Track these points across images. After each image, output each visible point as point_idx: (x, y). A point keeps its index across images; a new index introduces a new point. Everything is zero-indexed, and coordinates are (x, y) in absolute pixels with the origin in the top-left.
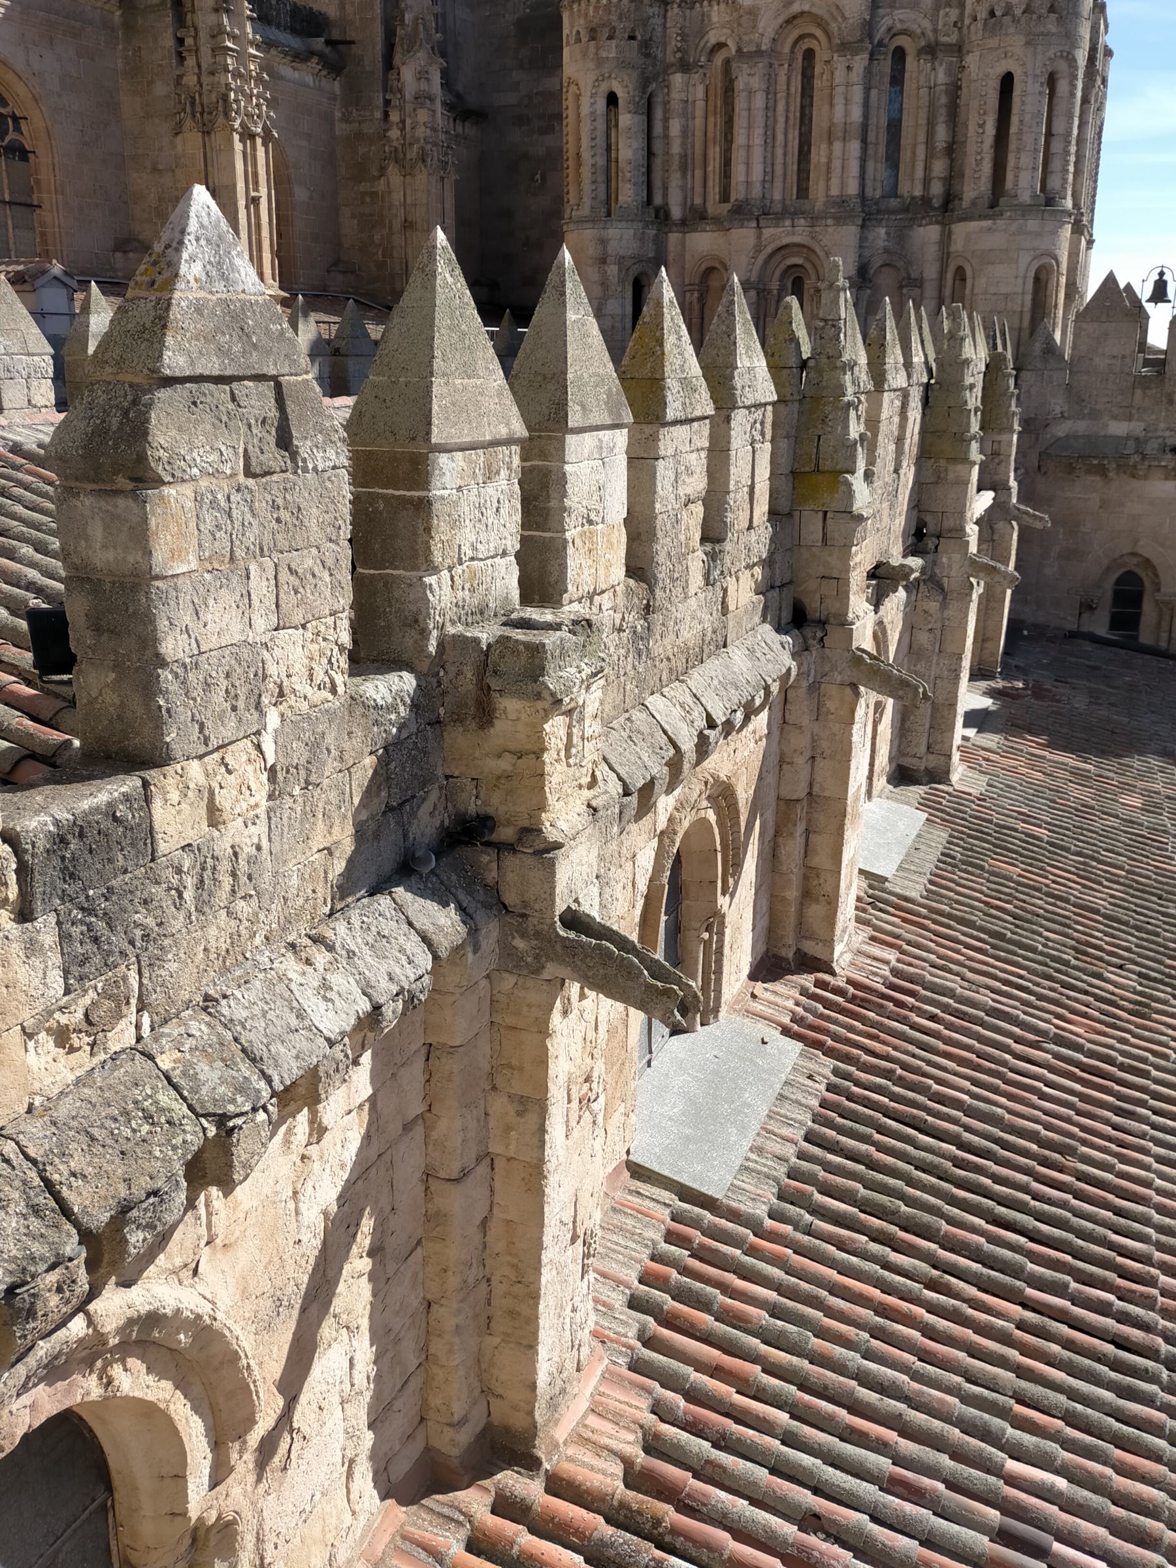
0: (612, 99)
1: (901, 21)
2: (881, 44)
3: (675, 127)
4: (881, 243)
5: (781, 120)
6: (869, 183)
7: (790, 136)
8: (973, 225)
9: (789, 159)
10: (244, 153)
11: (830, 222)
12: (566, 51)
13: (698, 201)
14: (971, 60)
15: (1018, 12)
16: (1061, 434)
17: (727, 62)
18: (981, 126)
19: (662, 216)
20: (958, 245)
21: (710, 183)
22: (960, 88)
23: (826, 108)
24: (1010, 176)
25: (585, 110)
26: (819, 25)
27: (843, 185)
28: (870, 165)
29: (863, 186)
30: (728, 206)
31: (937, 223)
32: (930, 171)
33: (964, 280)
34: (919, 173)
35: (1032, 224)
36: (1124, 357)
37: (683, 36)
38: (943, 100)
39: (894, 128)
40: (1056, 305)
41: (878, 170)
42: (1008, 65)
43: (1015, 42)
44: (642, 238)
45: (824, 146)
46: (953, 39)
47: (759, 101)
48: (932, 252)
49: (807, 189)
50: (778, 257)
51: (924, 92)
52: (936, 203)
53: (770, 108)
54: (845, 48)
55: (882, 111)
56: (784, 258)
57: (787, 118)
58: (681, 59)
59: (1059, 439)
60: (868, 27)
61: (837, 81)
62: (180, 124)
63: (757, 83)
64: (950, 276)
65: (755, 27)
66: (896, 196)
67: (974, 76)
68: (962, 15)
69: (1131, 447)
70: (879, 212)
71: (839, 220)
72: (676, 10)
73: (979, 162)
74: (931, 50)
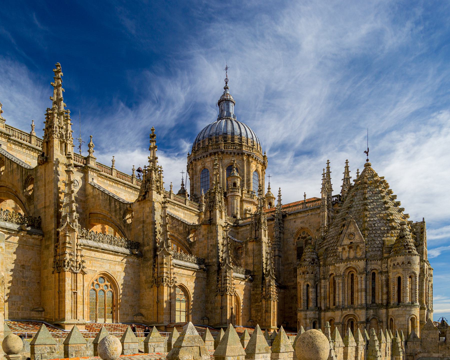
3: (322, 291)
4: (372, 314)
6: (368, 301)
7: (349, 292)
8: (394, 309)
9: (349, 296)
11: (358, 309)
13: (328, 306)
14: (390, 274)
18: (394, 288)
19: (320, 309)
20: (390, 313)
21: (331, 302)
22: (389, 280)
23: (357, 285)
24: (402, 298)
25: (302, 288)
27: (361, 301)
30: (335, 306)
31: (385, 309)
33: (392, 321)
34: (380, 298)
37: (324, 273)
38: (385, 283)
39: (374, 289)
40: (417, 327)
41: (370, 298)
42: (400, 275)
43: (400, 270)
44: (315, 314)
45: (356, 293)
46: (386, 270)
47: (341, 285)
48: (384, 315)
50: (347, 317)
52: (385, 304)
54: (361, 273)
55: (370, 286)
56: (348, 317)
57: (348, 288)
58: (323, 277)
60: (365, 269)
61: (359, 280)
63: (340, 281)
64: (389, 320)
65: (339, 270)
66: (375, 303)
67: (391, 278)
68: (388, 265)
71: (361, 309)
72: (322, 267)
74: (381, 273)
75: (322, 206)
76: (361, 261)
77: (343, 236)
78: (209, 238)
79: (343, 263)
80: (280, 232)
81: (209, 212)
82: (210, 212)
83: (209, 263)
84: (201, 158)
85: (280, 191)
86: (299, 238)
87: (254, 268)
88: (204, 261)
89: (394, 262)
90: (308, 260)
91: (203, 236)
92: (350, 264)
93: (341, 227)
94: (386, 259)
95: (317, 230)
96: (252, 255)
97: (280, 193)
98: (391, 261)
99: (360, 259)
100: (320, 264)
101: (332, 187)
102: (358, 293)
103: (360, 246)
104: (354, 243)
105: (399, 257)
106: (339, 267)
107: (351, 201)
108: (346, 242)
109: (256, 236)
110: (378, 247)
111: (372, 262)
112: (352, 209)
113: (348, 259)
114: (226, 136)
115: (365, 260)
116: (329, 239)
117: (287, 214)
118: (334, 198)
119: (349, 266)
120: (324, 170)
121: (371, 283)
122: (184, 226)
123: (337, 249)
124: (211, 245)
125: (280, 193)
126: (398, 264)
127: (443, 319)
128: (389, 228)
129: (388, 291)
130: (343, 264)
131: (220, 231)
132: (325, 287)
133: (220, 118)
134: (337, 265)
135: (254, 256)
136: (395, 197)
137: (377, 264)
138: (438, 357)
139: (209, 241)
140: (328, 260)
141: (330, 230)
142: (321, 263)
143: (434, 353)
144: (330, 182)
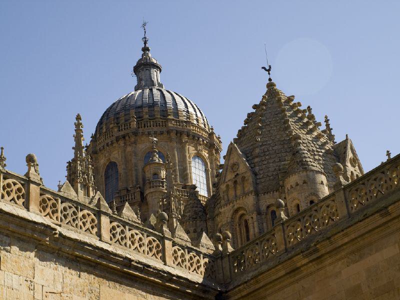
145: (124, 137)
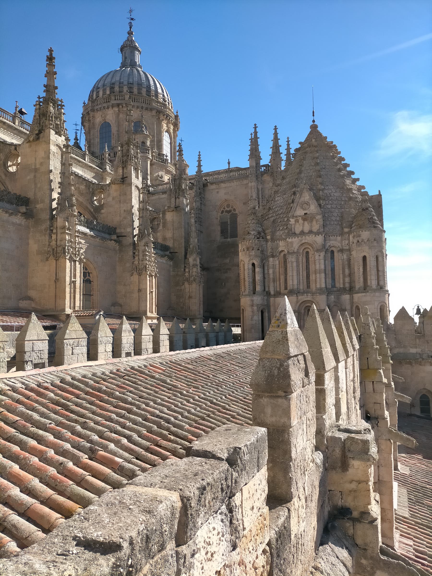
0: (253, 265)
1: (332, 244)
2: (327, 249)
3: (271, 271)
5: (301, 269)
6: (327, 284)
7: (304, 273)
9: (304, 278)
10: (150, 280)
11: (318, 294)
12: (240, 254)
13: (278, 289)
14: (354, 253)
15: (366, 241)
16: (395, 353)
17: (285, 255)
18: (359, 269)
19: (268, 294)
21: (281, 285)
23: (314, 265)
25: (246, 267)
26: (310, 245)
28: (327, 280)
29: (326, 285)
31: (348, 294)
32: (345, 281)
35: (377, 294)
36: (411, 330)
37: (272, 249)
38: (346, 263)
39: (333, 270)
41: (329, 281)
42: (365, 254)
43: (366, 248)
44: (263, 299)
45: (314, 275)
46: (347, 248)
47: (295, 264)
49: (310, 286)
51: (340, 261)
52: (347, 289)
53: (298, 266)
54: (318, 251)
58: (272, 254)
59: (395, 354)
60: (324, 246)
62: (133, 273)
63: (294, 260)
64: (354, 308)
67: (355, 257)
69: (418, 356)
70: (331, 292)
71: (320, 294)
72: (270, 243)
73: (359, 278)
74: (341, 251)
75: (250, 176)
76: (318, 236)
77: (296, 205)
78: (121, 201)
79: (296, 237)
80: (201, 203)
81: (121, 168)
82: (123, 168)
83: (122, 233)
84: (100, 109)
85: (199, 155)
86: (222, 212)
87: (174, 244)
88: (115, 231)
89: (358, 238)
90: (252, 233)
91: (113, 199)
92: (306, 239)
93: (291, 196)
94: (347, 235)
95: (244, 204)
96: (172, 228)
97: (199, 158)
98: (354, 237)
99: (318, 233)
100: (266, 239)
101: (260, 155)
102: (316, 274)
103: (317, 218)
104: (309, 214)
105: (364, 232)
106: (292, 243)
107: (300, 165)
108: (300, 212)
109: (176, 205)
110: (336, 220)
111: (331, 237)
112: (302, 175)
113: (302, 233)
114: (132, 86)
115: (323, 235)
116: (276, 209)
117: (208, 182)
118: (263, 168)
119: (303, 241)
120: (251, 134)
121: (330, 263)
122: (86, 183)
123: (288, 220)
124: (125, 211)
125: (199, 158)
126: (363, 240)
127: (418, 307)
128: (347, 199)
129: (350, 273)
130: (296, 239)
131: (135, 194)
132: (274, 267)
133: (123, 65)
134: (289, 240)
135: (173, 229)
136: (347, 165)
137: (336, 240)
138: (417, 353)
139: (122, 205)
140: (277, 234)
141: (277, 199)
142: (269, 237)
143: (412, 348)
144: (258, 149)
145: (118, 105)
